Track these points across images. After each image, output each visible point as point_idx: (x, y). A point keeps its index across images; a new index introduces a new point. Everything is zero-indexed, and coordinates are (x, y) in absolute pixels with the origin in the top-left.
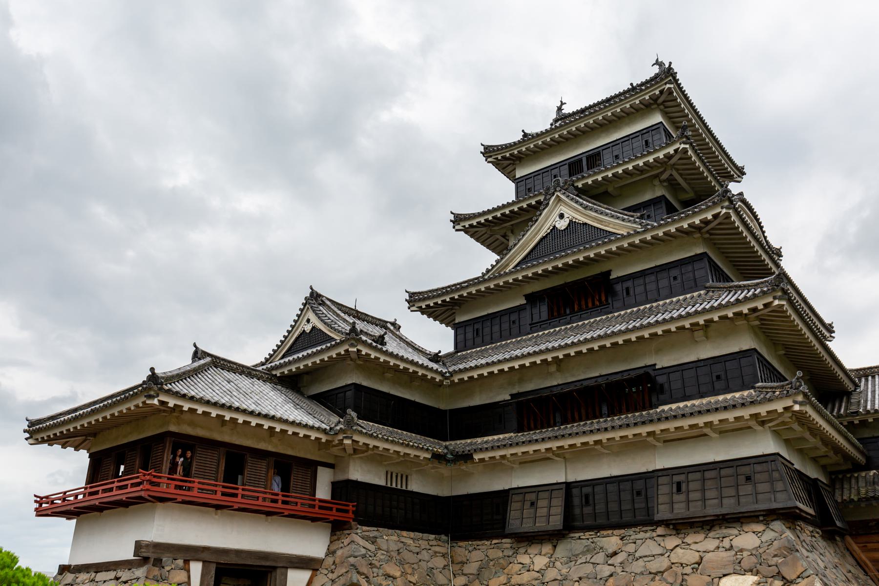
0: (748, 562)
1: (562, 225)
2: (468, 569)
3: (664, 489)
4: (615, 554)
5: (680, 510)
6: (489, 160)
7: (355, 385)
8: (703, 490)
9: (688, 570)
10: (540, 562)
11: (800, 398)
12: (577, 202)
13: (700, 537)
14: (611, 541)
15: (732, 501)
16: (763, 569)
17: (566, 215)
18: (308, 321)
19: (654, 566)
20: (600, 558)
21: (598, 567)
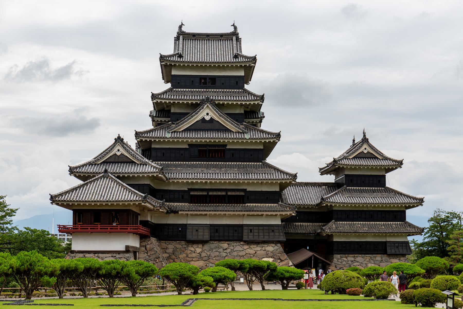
0: (270, 254)
1: (208, 118)
2: (167, 251)
3: (245, 231)
4: (226, 249)
5: (251, 238)
6: (163, 63)
7: (149, 184)
8: (259, 233)
9: (252, 256)
10: (199, 250)
11: (295, 212)
12: (217, 112)
13: (255, 246)
14: (225, 245)
15: (268, 237)
16: (275, 257)
17: (210, 114)
18: (119, 150)
19: (241, 254)
20: (221, 250)
21: (221, 253)
